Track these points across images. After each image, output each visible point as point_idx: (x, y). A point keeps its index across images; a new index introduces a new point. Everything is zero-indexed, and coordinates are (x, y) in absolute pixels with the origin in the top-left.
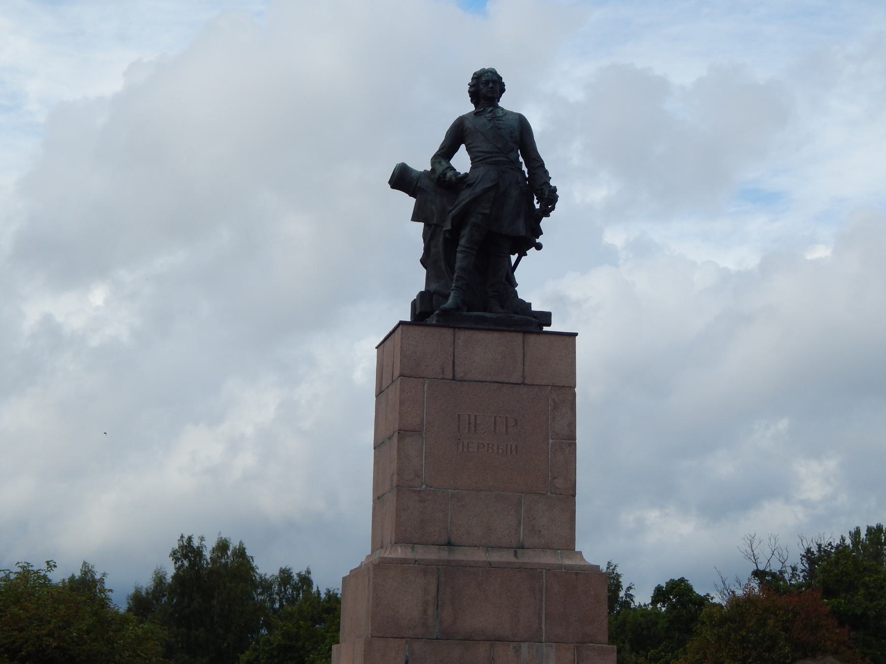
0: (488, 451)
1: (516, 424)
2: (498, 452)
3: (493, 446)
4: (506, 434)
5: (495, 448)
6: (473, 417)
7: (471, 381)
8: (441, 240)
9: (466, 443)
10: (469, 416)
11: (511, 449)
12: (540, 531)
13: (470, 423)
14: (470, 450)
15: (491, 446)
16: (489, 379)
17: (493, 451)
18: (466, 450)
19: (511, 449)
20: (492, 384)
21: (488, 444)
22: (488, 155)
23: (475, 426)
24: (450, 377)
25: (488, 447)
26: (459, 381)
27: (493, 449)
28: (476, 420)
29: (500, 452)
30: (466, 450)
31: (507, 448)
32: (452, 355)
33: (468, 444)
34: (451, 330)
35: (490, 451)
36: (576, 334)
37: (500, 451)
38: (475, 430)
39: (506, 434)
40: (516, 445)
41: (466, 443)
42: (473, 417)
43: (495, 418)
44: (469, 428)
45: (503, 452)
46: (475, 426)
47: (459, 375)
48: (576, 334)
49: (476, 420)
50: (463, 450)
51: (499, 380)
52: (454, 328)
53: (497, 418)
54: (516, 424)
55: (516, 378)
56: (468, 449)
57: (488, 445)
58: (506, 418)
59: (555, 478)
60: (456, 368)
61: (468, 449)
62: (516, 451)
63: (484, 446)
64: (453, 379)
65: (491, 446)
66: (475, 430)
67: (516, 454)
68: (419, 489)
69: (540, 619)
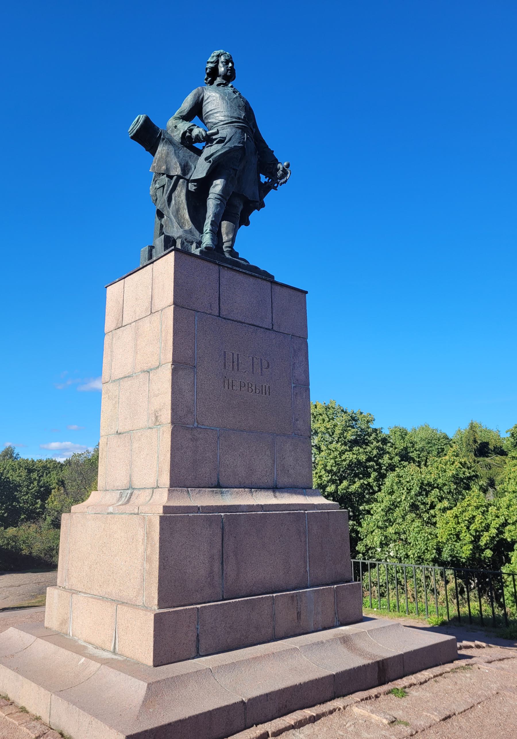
0: (248, 390)
1: (268, 366)
2: (256, 393)
3: (252, 386)
4: (262, 375)
5: (253, 388)
6: (235, 356)
7: (233, 320)
8: (184, 191)
9: (230, 381)
10: (233, 354)
11: (265, 390)
12: (288, 471)
13: (233, 362)
14: (234, 388)
15: (250, 386)
16: (247, 321)
17: (252, 392)
18: (230, 387)
19: (265, 390)
20: (250, 326)
21: (248, 383)
22: (234, 120)
23: (238, 365)
24: (217, 313)
25: (248, 387)
26: (224, 318)
27: (252, 389)
28: (238, 359)
29: (257, 392)
30: (230, 387)
31: (262, 389)
32: (218, 292)
33: (232, 382)
34: (217, 267)
35: (250, 390)
36: (306, 292)
37: (258, 391)
38: (238, 370)
39: (262, 375)
40: (269, 387)
41: (230, 381)
42: (235, 356)
43: (253, 358)
44: (233, 366)
45: (259, 392)
46: (238, 365)
47: (224, 313)
48: (306, 292)
49: (238, 359)
50: (228, 388)
51: (255, 324)
52: (219, 265)
53: (254, 359)
54: (268, 366)
55: (267, 324)
56: (232, 387)
57: (248, 385)
58: (261, 359)
59: (297, 420)
60: (221, 305)
61: (232, 387)
62: (269, 393)
63: (245, 386)
64: (219, 316)
65: (250, 386)
66: (238, 370)
67: (269, 395)
68: (191, 426)
69: (305, 562)
